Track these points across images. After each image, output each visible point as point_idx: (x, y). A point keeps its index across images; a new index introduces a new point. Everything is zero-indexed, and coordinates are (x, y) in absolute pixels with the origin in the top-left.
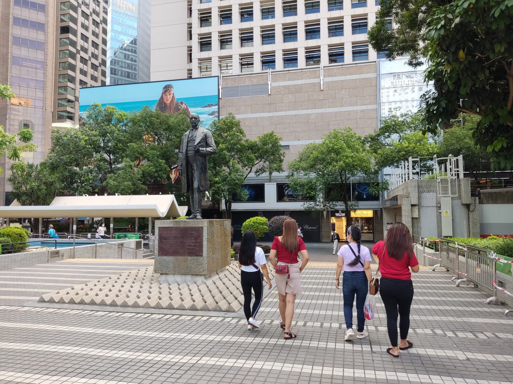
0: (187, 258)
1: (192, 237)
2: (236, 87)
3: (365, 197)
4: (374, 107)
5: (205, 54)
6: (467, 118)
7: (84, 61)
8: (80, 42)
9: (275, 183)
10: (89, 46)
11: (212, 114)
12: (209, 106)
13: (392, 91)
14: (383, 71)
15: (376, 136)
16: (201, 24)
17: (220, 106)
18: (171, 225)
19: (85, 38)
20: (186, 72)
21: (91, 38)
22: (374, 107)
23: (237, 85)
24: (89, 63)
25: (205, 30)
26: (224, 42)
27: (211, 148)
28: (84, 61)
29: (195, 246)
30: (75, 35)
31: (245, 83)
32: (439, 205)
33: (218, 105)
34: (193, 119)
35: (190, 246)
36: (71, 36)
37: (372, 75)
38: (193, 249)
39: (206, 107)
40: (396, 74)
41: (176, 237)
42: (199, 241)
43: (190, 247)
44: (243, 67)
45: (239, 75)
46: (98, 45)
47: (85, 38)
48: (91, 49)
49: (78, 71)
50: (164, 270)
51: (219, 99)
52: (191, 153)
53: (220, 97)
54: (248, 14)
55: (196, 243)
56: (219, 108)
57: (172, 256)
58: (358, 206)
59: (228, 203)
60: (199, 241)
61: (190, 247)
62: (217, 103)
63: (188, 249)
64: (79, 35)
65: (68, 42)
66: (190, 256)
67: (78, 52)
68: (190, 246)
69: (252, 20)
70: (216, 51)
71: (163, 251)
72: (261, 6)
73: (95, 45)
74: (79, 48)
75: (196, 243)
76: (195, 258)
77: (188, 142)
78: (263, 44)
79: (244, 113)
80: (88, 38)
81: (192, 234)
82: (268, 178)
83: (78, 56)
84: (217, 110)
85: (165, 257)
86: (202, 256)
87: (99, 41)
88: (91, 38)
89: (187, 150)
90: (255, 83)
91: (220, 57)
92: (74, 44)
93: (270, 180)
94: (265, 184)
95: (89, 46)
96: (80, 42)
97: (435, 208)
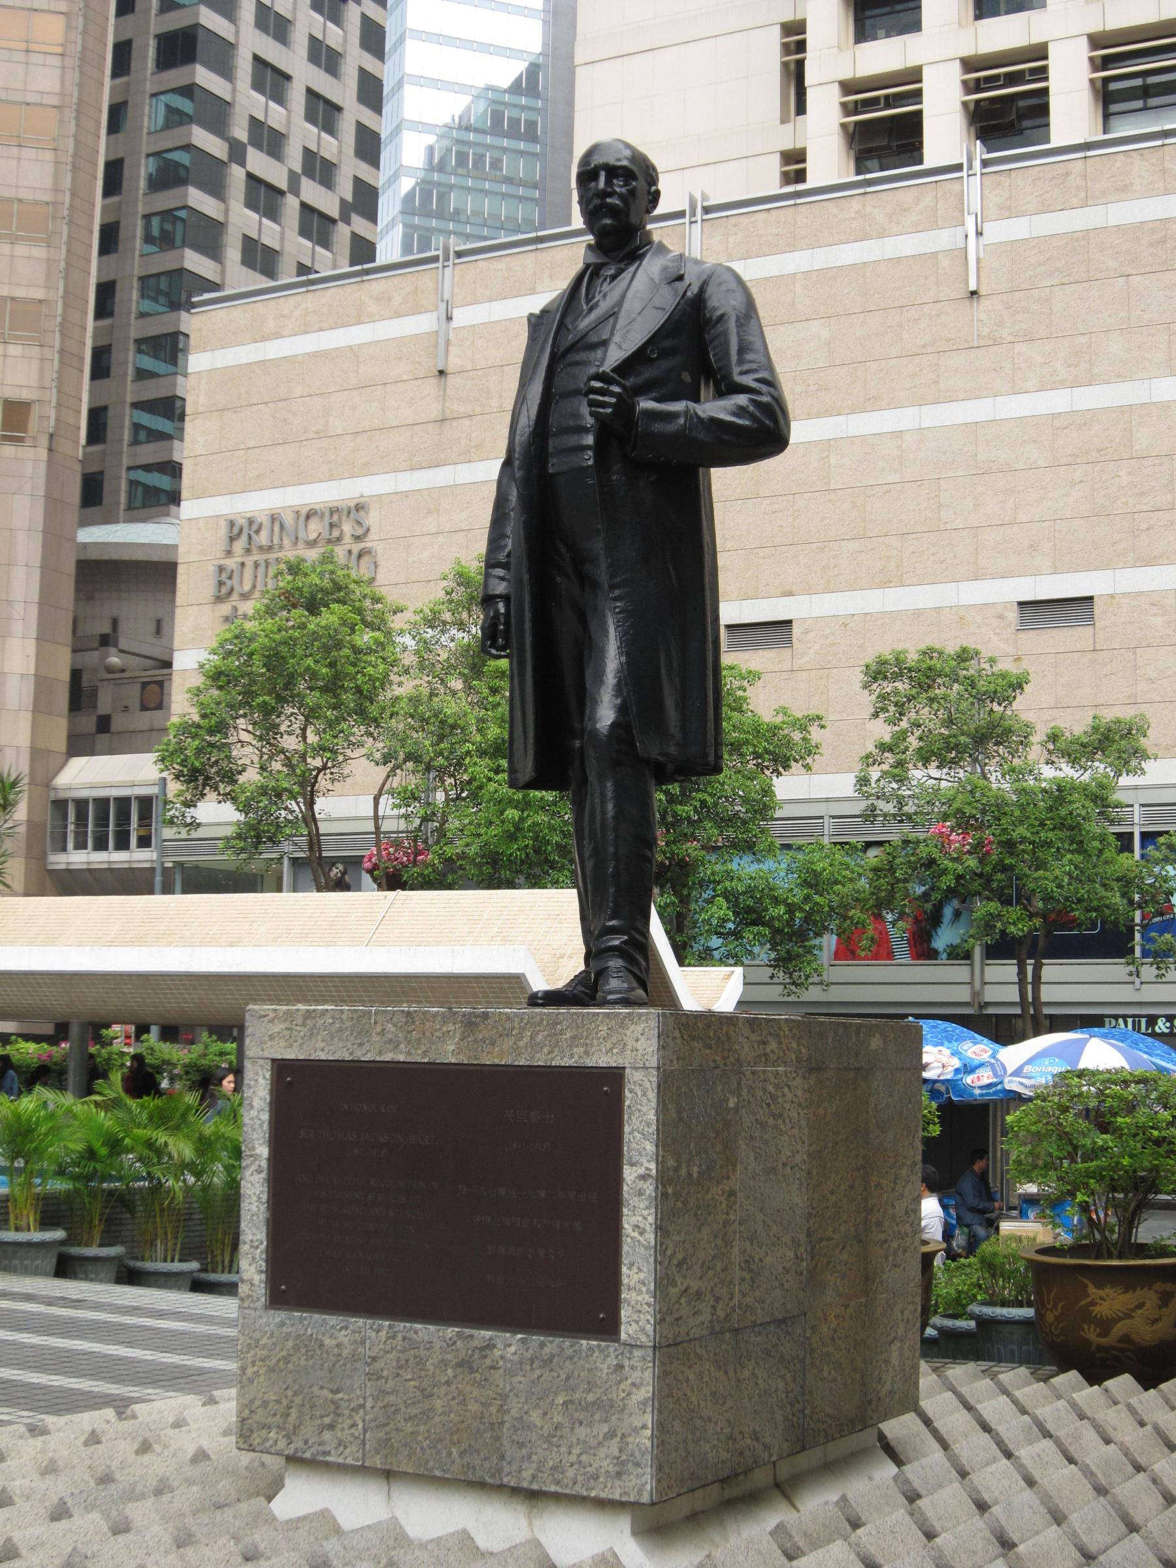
0: (490, 1346)
7: (265, 198)
8: (249, 103)
10: (288, 117)
19: (271, 79)
20: (773, 168)
21: (304, 75)
24: (291, 204)
27: (742, 399)
28: (265, 198)
30: (226, 71)
36: (204, 77)
44: (1114, 108)
45: (1088, 146)
46: (339, 109)
47: (271, 79)
48: (303, 134)
49: (233, 253)
50: (309, 1431)
64: (244, 67)
65: (186, 106)
67: (237, 153)
73: (322, 111)
74: (241, 133)
76: (553, 1344)
79: (1121, 377)
80: (288, 78)
83: (237, 174)
87: (343, 92)
88: (304, 75)
92: (216, 113)
95: (288, 117)
96: (249, 103)
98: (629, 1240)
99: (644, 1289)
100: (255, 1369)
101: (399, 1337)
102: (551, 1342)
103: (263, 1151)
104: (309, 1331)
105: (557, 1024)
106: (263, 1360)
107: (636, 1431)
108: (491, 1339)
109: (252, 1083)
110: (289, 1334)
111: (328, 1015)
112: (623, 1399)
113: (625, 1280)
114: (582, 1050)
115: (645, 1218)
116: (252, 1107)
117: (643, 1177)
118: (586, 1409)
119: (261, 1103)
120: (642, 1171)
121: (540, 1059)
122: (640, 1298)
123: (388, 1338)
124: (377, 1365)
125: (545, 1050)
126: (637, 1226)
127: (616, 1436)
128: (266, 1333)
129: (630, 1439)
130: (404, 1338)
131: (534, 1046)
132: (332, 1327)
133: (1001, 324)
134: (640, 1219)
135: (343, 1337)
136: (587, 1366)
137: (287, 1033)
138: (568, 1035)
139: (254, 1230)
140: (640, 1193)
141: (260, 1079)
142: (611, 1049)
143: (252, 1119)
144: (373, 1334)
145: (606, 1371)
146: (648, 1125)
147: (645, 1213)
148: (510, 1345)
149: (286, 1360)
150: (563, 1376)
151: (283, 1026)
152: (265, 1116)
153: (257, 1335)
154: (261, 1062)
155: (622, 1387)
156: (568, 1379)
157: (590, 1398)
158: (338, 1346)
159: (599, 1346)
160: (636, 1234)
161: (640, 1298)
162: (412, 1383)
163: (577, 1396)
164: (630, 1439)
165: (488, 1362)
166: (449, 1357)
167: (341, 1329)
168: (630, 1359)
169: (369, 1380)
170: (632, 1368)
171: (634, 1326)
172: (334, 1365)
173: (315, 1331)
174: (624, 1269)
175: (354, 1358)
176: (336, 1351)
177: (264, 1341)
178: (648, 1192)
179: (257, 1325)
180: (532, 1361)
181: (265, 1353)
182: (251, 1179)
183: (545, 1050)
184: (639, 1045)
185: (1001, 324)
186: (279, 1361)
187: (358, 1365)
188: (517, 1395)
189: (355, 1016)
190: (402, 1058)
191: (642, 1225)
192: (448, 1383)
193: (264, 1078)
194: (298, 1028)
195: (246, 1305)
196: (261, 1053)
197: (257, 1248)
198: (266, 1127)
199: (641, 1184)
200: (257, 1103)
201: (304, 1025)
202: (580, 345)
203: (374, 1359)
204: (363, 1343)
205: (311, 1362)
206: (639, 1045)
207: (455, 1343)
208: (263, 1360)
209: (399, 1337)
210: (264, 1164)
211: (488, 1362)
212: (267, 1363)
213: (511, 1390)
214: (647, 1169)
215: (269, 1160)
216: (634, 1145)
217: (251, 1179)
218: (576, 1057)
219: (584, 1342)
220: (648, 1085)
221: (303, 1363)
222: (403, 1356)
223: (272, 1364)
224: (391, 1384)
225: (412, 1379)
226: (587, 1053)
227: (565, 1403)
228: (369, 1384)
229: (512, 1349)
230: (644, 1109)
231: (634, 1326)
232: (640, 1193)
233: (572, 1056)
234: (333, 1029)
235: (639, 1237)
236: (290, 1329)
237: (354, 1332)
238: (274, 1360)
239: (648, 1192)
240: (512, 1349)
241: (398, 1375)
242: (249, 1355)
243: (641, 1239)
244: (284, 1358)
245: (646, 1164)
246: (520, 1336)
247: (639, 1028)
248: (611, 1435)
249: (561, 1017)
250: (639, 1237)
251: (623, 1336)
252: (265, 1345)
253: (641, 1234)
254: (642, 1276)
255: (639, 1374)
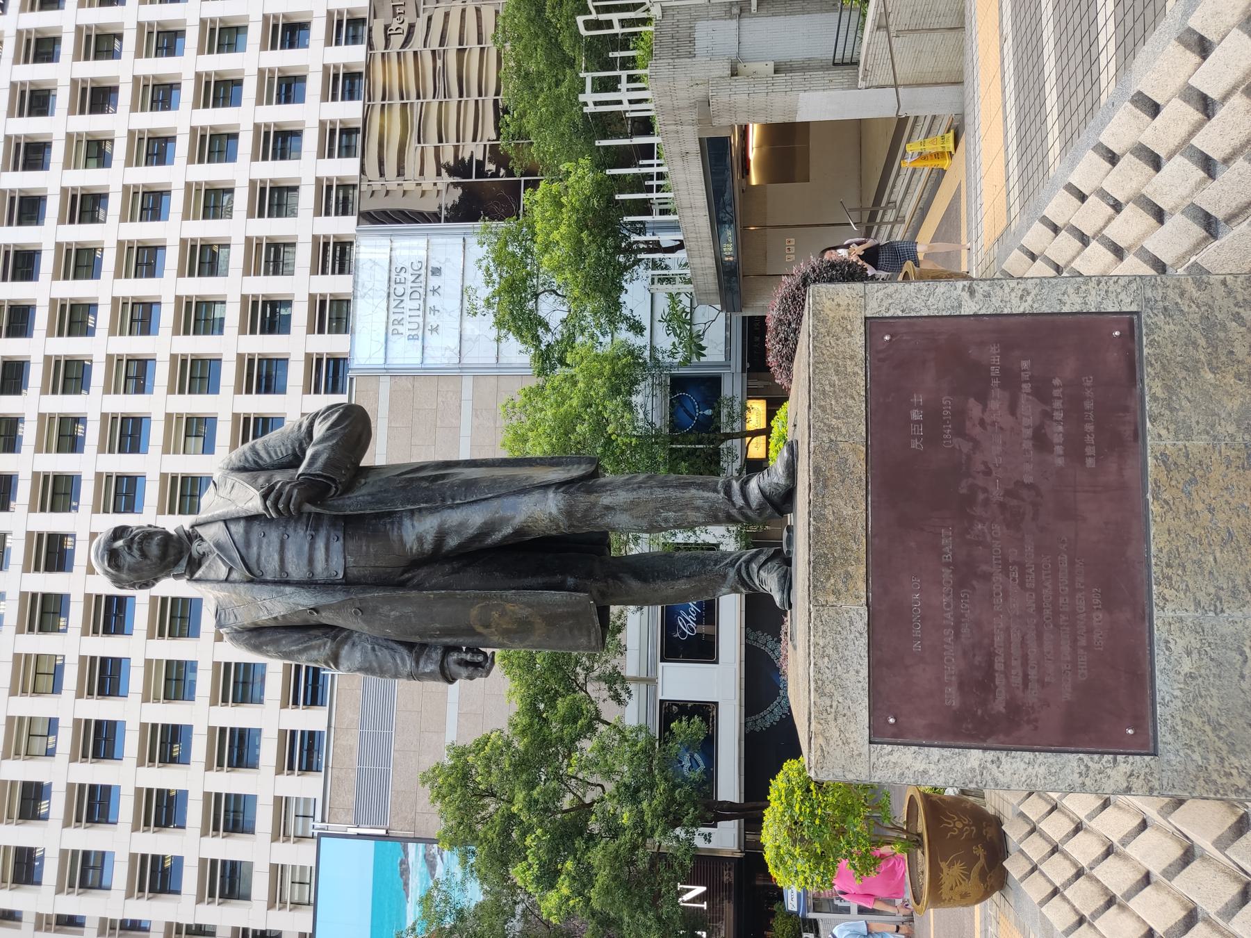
0: (1163, 458)
1: (960, 415)
2: (359, 778)
3: (708, 412)
4: (467, 383)
5: (260, 885)
6: (511, 130)
9: (661, 665)
11: (432, 866)
12: (404, 872)
13: (432, 340)
14: (378, 360)
15: (537, 347)
16: (170, 892)
17: (410, 834)
18: (856, 614)
22: (467, 383)
23: (353, 775)
25: (190, 879)
26: (236, 822)
29: (1042, 393)
31: (351, 749)
32: (735, 11)
33: (405, 840)
34: (120, 543)
35: (1041, 440)
37: (385, 385)
38: (1074, 404)
39: (406, 884)
40: (391, 328)
41: (967, 575)
42: (993, 355)
43: (1057, 432)
51: (386, 837)
52: (330, 557)
53: (383, 832)
54: (174, 741)
55: (1010, 380)
56: (417, 840)
57: (1143, 616)
58: (732, 399)
59: (715, 812)
60: (993, 355)
61: (1057, 432)
62: (398, 845)
63: (1075, 451)
66: (1138, 434)
68: (1041, 440)
69: (189, 728)
70: (255, 850)
71: (1105, 711)
72: (157, 699)
75: (1010, 380)
76: (1152, 386)
77: (255, 578)
78: (261, 702)
81: (933, 417)
82: (643, 686)
84: (421, 846)
85: (1167, 687)
86: (1130, 323)
89: (309, 584)
90: (357, 717)
91: (275, 838)
93: (650, 681)
94: (660, 697)
97: (745, 21)
98: (1035, 305)
99: (1084, 288)
100: (1234, 772)
101: (1168, 571)
102: (1150, 388)
103: (975, 757)
104: (1177, 693)
105: (824, 391)
106: (1222, 759)
107: (1230, 293)
108: (1156, 458)
109: (898, 771)
110: (1184, 721)
111: (820, 663)
112: (1198, 307)
113: (1076, 308)
114: (849, 362)
115: (1013, 290)
116: (925, 772)
117: (972, 292)
118: (1215, 347)
119: (920, 758)
120: (966, 295)
121: (859, 408)
122: (1093, 292)
123: (1171, 586)
124: (1205, 601)
125: (850, 402)
126: (1021, 298)
127: (1238, 313)
128: (1187, 755)
129: (1240, 298)
130: (1169, 565)
131: (847, 410)
132: (1168, 661)
133: (405, 818)
134: (1013, 295)
135: (1178, 648)
136: (1170, 346)
137: (840, 720)
138: (835, 378)
139: (1068, 771)
140: (987, 296)
141: (893, 758)
142: (849, 332)
143: (939, 771)
144: (1169, 606)
145: (1172, 327)
146: (920, 290)
147: (1007, 290)
148: (1160, 436)
149: (1217, 727)
150: (1184, 373)
151: (832, 723)
152: (935, 752)
153: (1191, 768)
154: (873, 759)
155: (1186, 309)
156: (1187, 370)
157: (1202, 342)
158: (1189, 654)
159: (1147, 335)
160: (1029, 299)
161: (1093, 292)
162: (1218, 555)
163: (1202, 357)
164: (1240, 298)
165: (1182, 461)
166: (1182, 508)
167: (1168, 649)
168: (1156, 301)
169: (1222, 611)
170: (1164, 298)
171: (1122, 296)
172: (1212, 660)
173: (1176, 686)
174: (1066, 309)
175: (1199, 630)
176: (1195, 656)
177: (1196, 757)
178: (987, 288)
179: (1180, 768)
180: (1172, 410)
181: (1212, 757)
182: (1008, 774)
183: (850, 402)
184: (844, 304)
185: (405, 818)
186: (1220, 738)
187: (1207, 626)
188: (1213, 426)
189: (820, 629)
190: (863, 570)
191: (1020, 293)
192: (1211, 510)
193: (891, 753)
194: (834, 704)
195: (1156, 784)
196: (864, 758)
197: (1087, 766)
198: (946, 752)
199: (979, 296)
200: (920, 766)
201: (831, 697)
202: (243, 551)
203: (1198, 604)
204: (1181, 620)
205: (1214, 691)
206: (844, 304)
207: (1165, 501)
208: (1222, 759)
209: (1168, 571)
210: (990, 755)
211: (1182, 461)
212: (1224, 754)
213: (1208, 433)
214: (963, 290)
215: (985, 749)
216: (941, 305)
217: (1008, 774)
218: (856, 369)
219: (1146, 351)
220: (880, 294)
221: (1216, 703)
222: (1189, 566)
223: (1225, 747)
224: (1223, 582)
225: (1213, 553)
226: (852, 358)
227: (1213, 370)
228: (1227, 611)
229: (1164, 432)
230: (905, 295)
231: (1122, 296)
232: (987, 296)
233: (855, 374)
234: (835, 656)
235: (1032, 295)
236: (1178, 720)
237: (1169, 631)
238: (1219, 744)
239: (987, 288)
240: (1164, 432)
241: (1210, 573)
242: (1219, 781)
243: (1034, 292)
244: (1214, 729)
245: (959, 291)
246: (1148, 425)
247: (828, 303)
248: (1237, 317)
249: (818, 386)
250: (1032, 295)
251: (1134, 308)
252: (1203, 758)
253: (1028, 294)
254: (1070, 291)
255: (1170, 291)
